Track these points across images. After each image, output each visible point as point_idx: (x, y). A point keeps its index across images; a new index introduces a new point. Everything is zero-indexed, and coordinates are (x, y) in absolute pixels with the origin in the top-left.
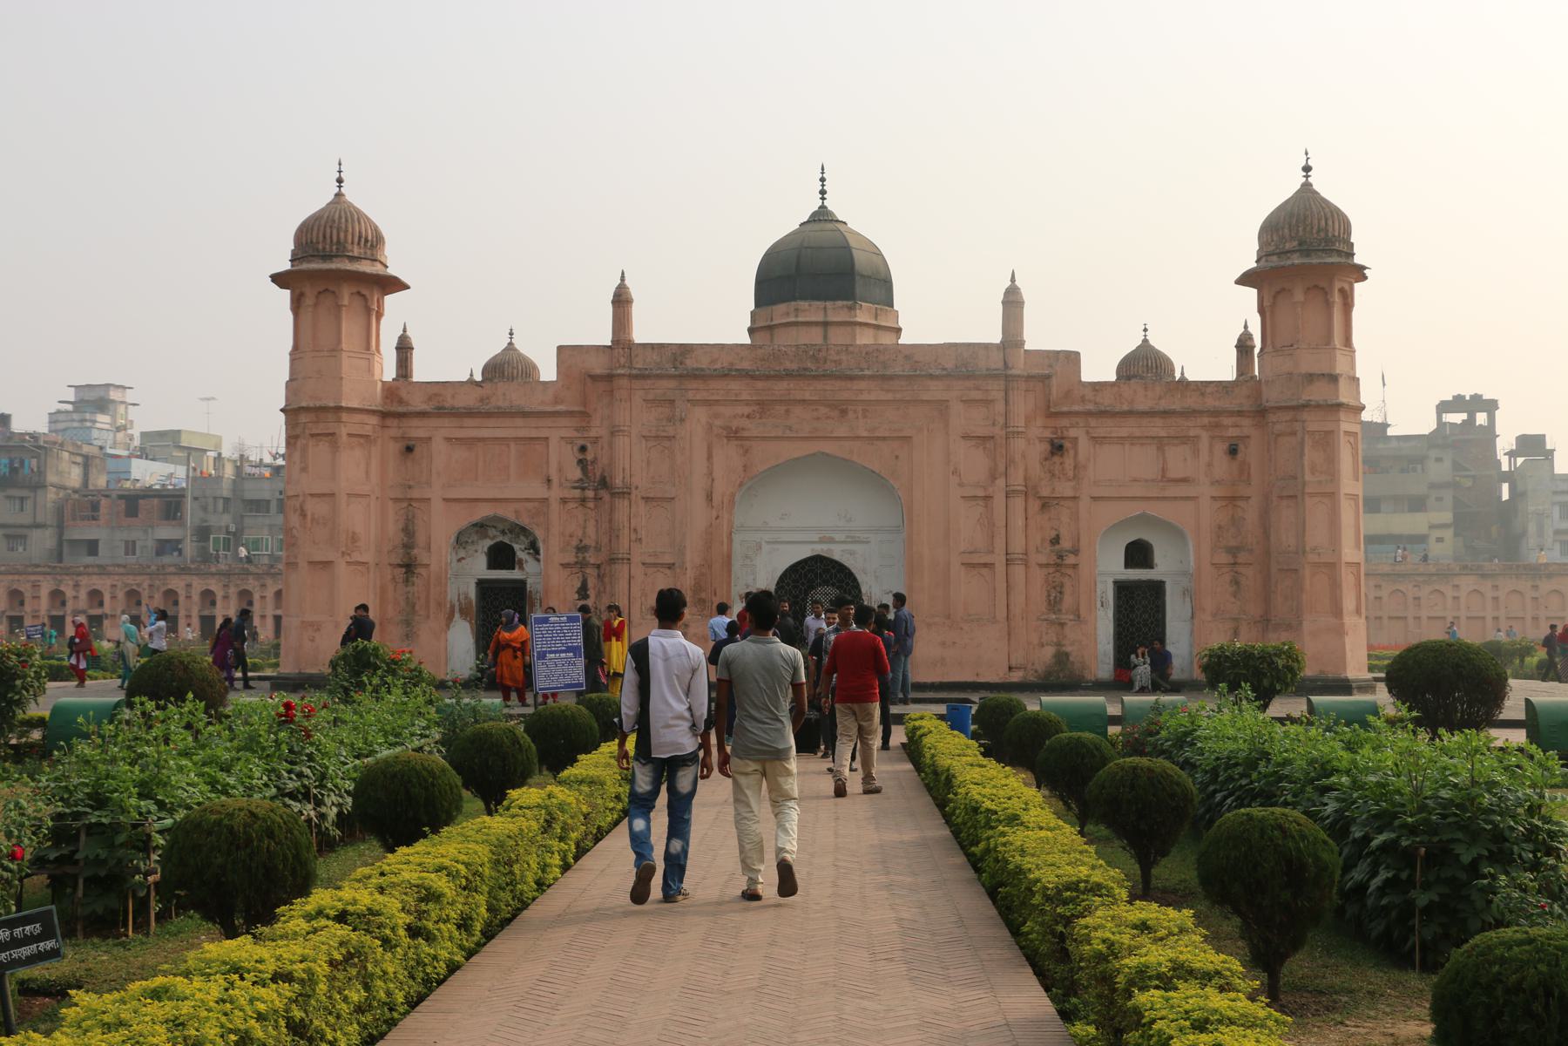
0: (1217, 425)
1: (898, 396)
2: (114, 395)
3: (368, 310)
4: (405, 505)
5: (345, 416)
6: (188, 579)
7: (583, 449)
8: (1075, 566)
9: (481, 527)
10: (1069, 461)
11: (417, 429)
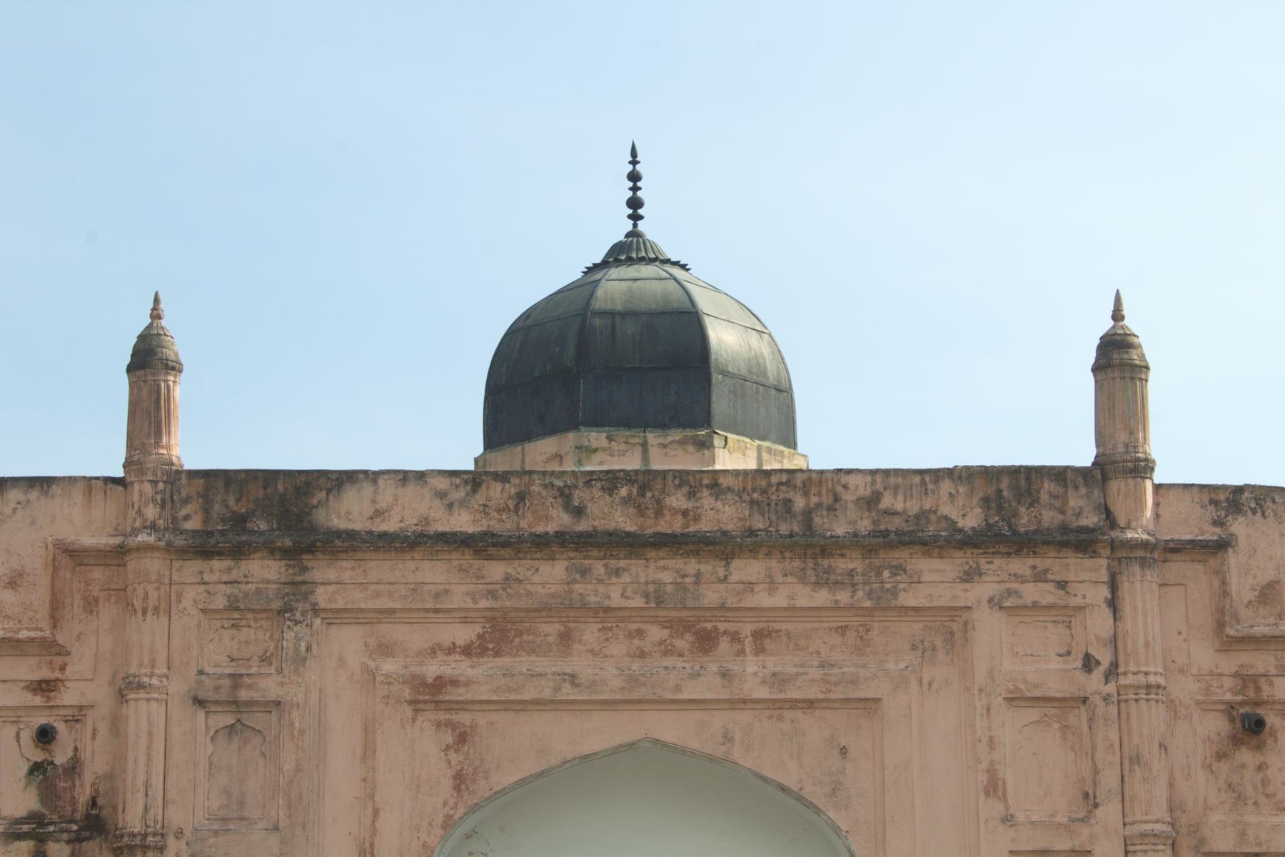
7: (45, 736)
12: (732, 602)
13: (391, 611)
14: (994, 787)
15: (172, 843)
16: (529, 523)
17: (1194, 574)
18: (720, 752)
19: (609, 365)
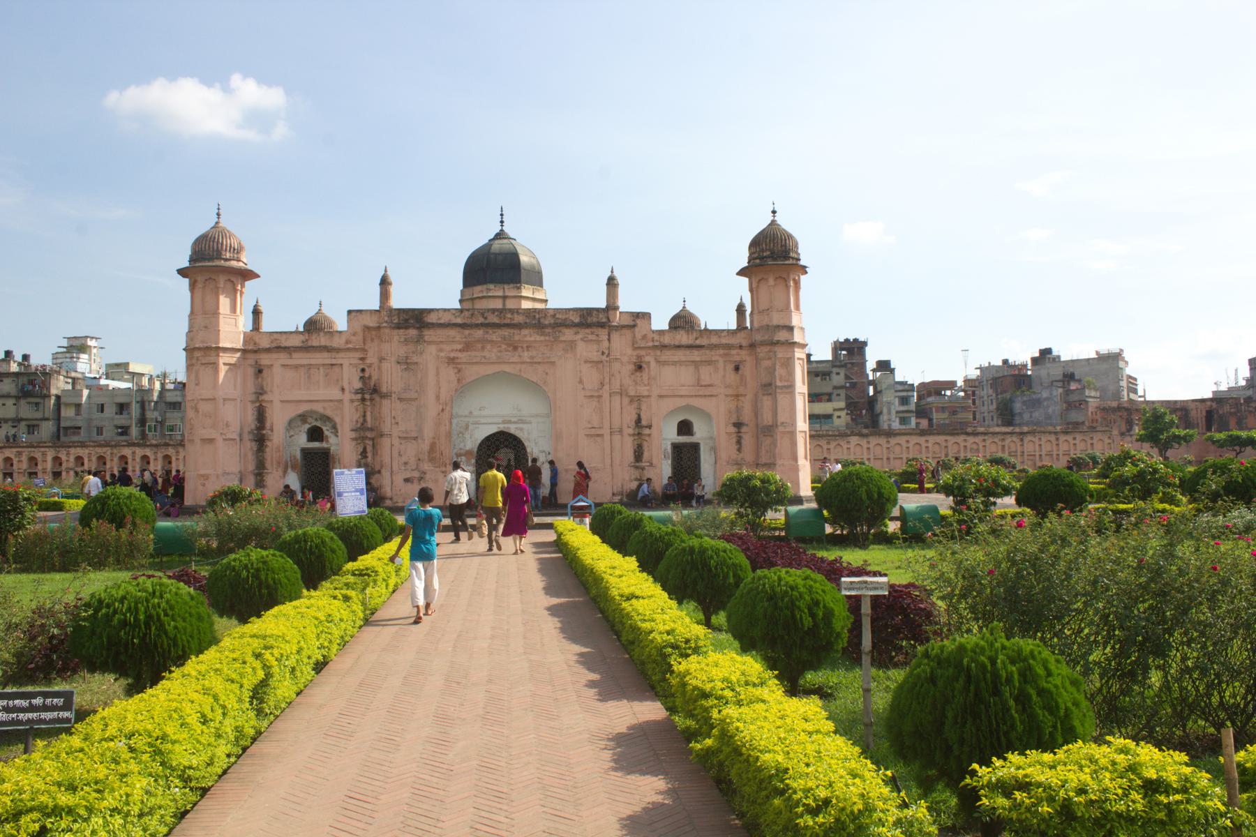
2: (91, 343)
3: (235, 291)
6: (134, 449)
7: (363, 370)
9: (303, 418)
10: (645, 375)
11: (265, 360)
14: (581, 382)
16: (474, 321)
17: (627, 332)
19: (495, 267)
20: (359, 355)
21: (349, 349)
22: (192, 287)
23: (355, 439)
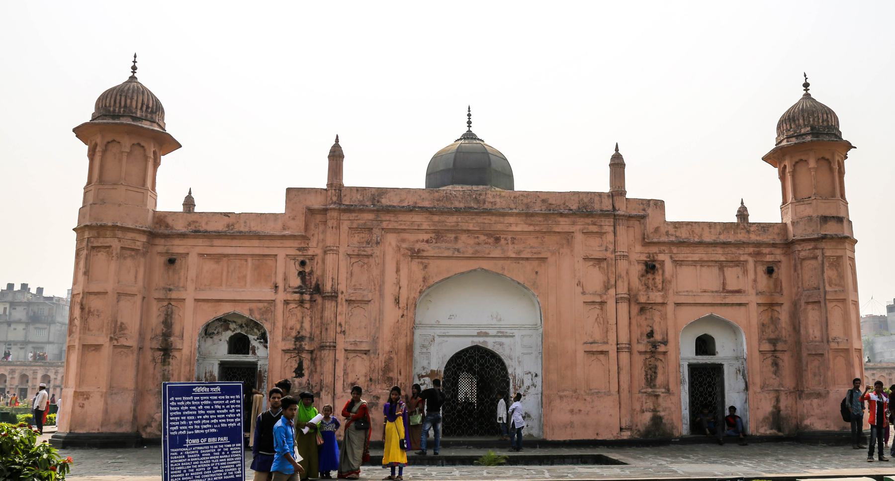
0: (758, 254)
1: (537, 228)
3: (146, 158)
4: (165, 303)
5: (119, 234)
8: (665, 353)
9: (224, 322)
11: (178, 247)
12: (505, 229)
13: (404, 230)
15: (340, 295)
18: (501, 272)
20: (296, 244)
21: (283, 237)
22: (91, 155)
23: (286, 351)
